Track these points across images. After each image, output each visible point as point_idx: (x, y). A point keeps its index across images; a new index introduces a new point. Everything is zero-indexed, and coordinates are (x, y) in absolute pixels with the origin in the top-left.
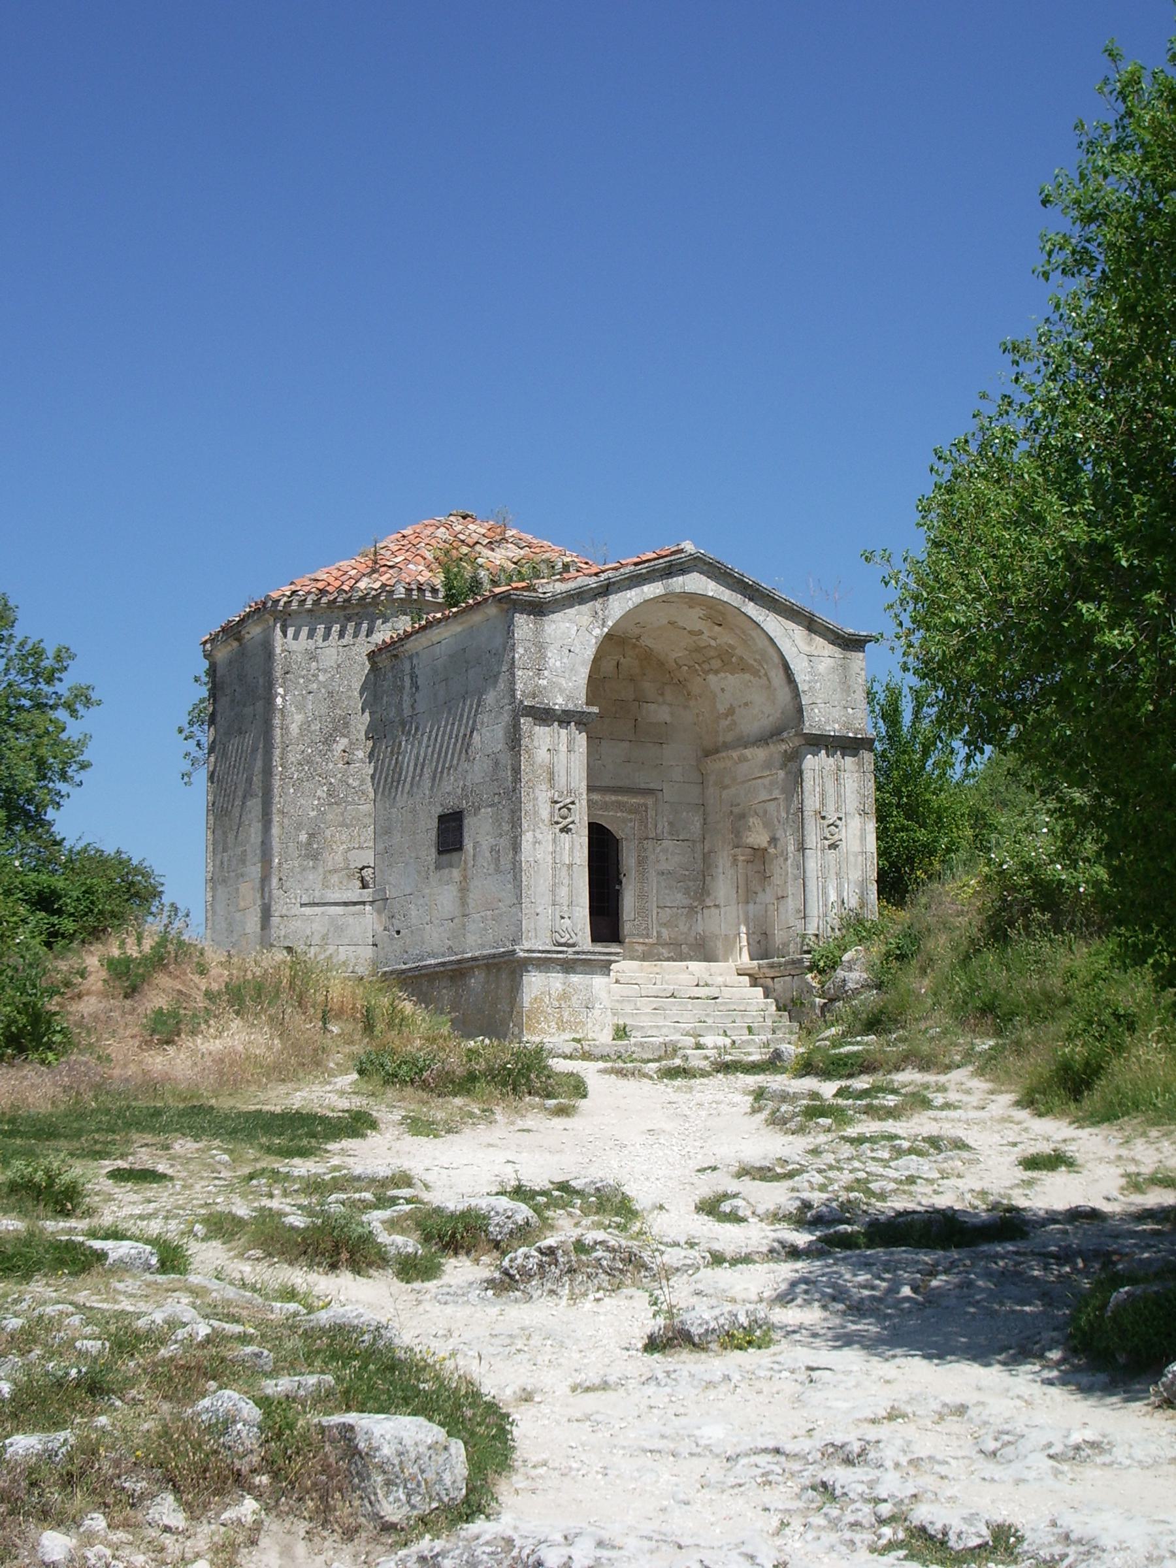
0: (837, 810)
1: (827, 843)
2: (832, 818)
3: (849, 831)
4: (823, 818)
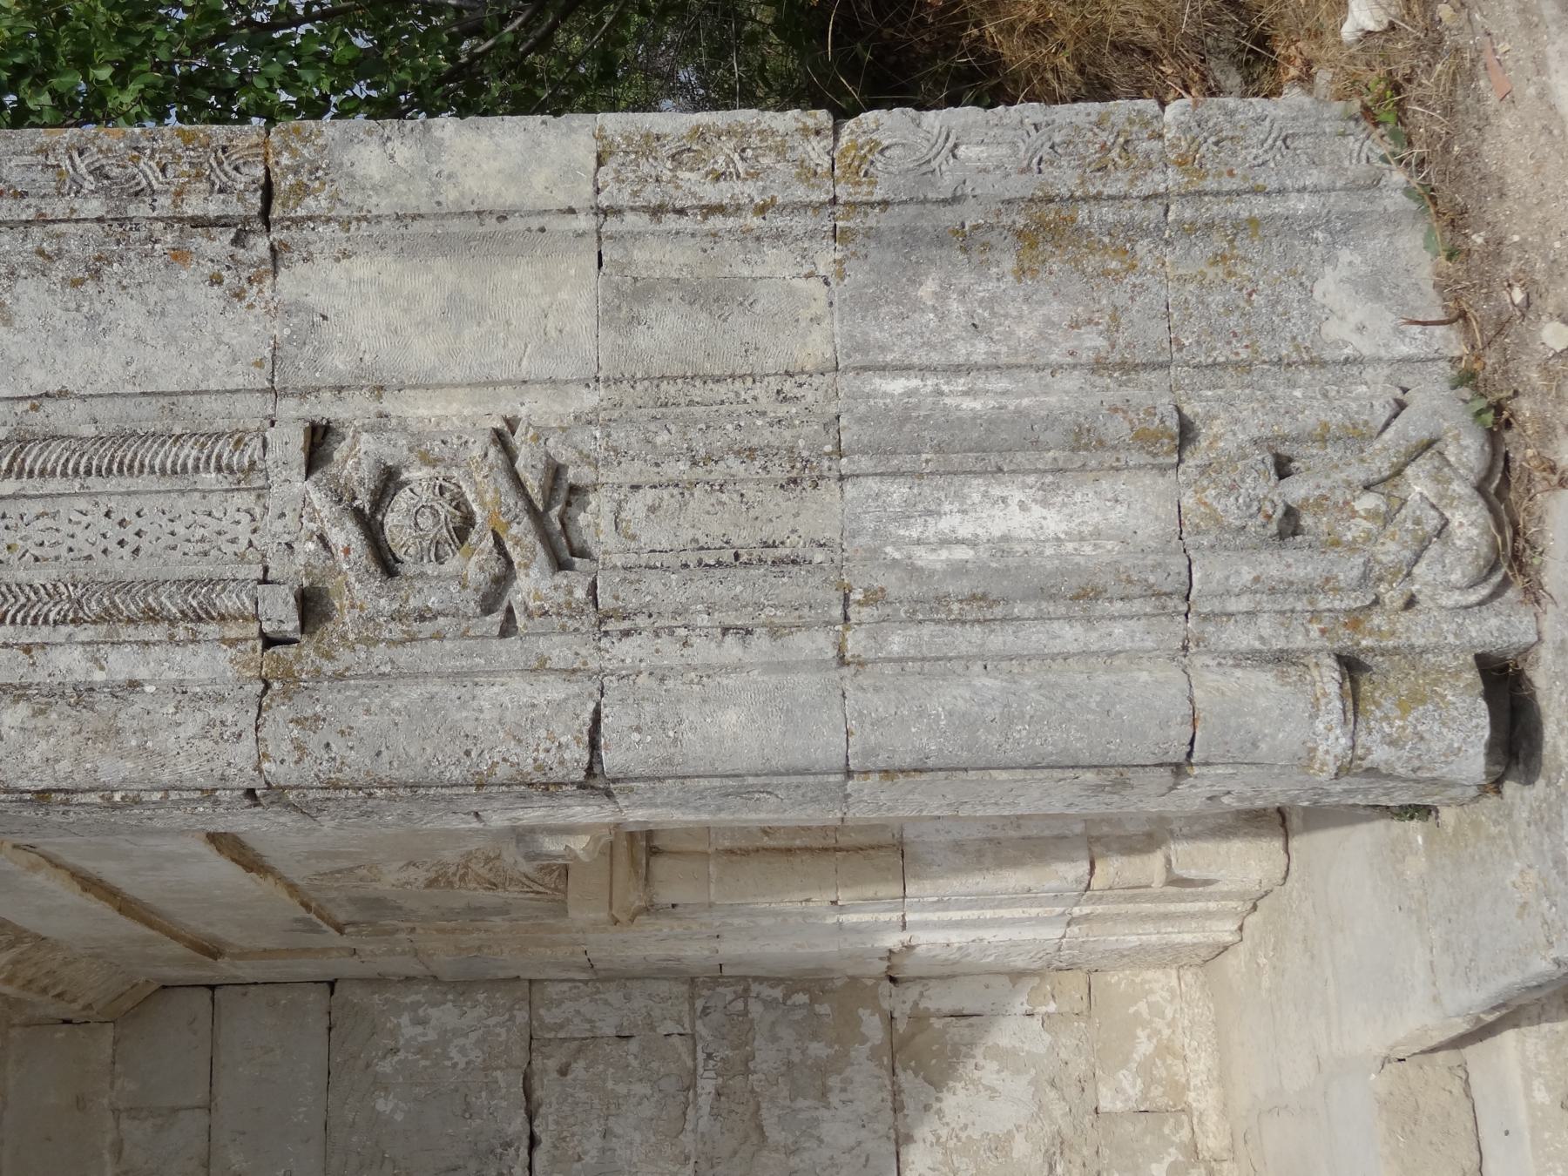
0: (246, 476)
1: (533, 583)
2: (299, 522)
3: (424, 352)
4: (312, 606)
